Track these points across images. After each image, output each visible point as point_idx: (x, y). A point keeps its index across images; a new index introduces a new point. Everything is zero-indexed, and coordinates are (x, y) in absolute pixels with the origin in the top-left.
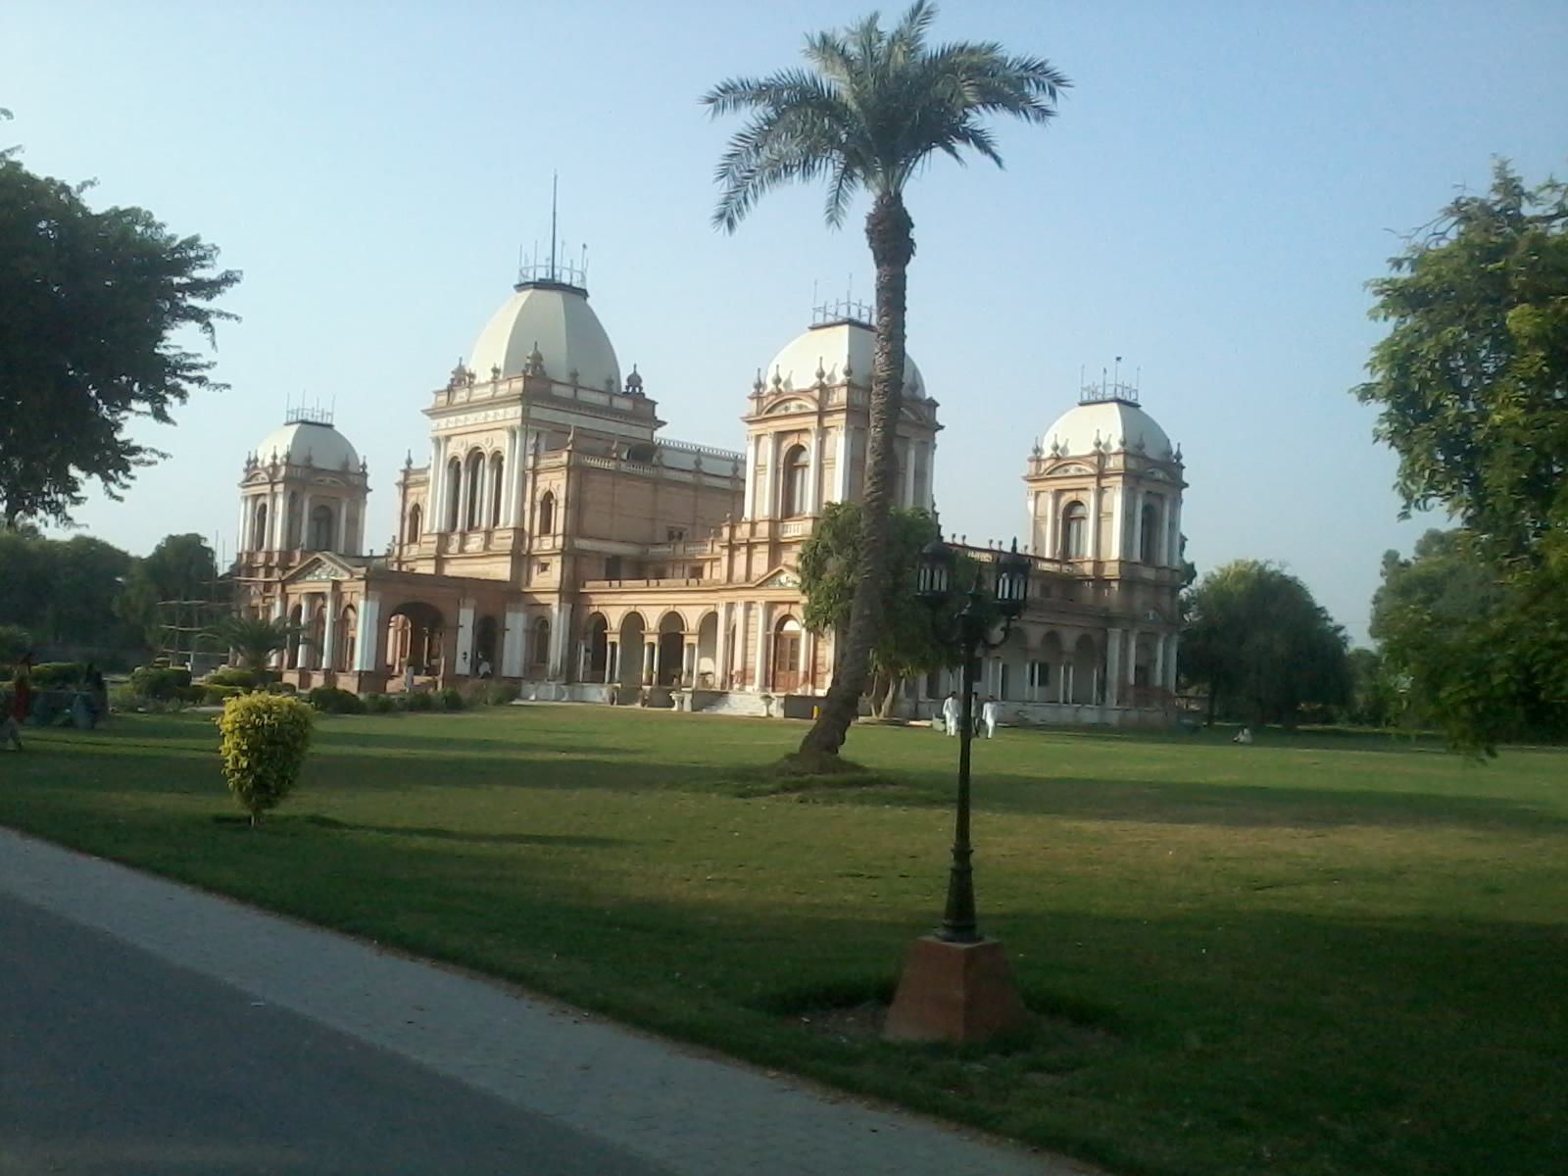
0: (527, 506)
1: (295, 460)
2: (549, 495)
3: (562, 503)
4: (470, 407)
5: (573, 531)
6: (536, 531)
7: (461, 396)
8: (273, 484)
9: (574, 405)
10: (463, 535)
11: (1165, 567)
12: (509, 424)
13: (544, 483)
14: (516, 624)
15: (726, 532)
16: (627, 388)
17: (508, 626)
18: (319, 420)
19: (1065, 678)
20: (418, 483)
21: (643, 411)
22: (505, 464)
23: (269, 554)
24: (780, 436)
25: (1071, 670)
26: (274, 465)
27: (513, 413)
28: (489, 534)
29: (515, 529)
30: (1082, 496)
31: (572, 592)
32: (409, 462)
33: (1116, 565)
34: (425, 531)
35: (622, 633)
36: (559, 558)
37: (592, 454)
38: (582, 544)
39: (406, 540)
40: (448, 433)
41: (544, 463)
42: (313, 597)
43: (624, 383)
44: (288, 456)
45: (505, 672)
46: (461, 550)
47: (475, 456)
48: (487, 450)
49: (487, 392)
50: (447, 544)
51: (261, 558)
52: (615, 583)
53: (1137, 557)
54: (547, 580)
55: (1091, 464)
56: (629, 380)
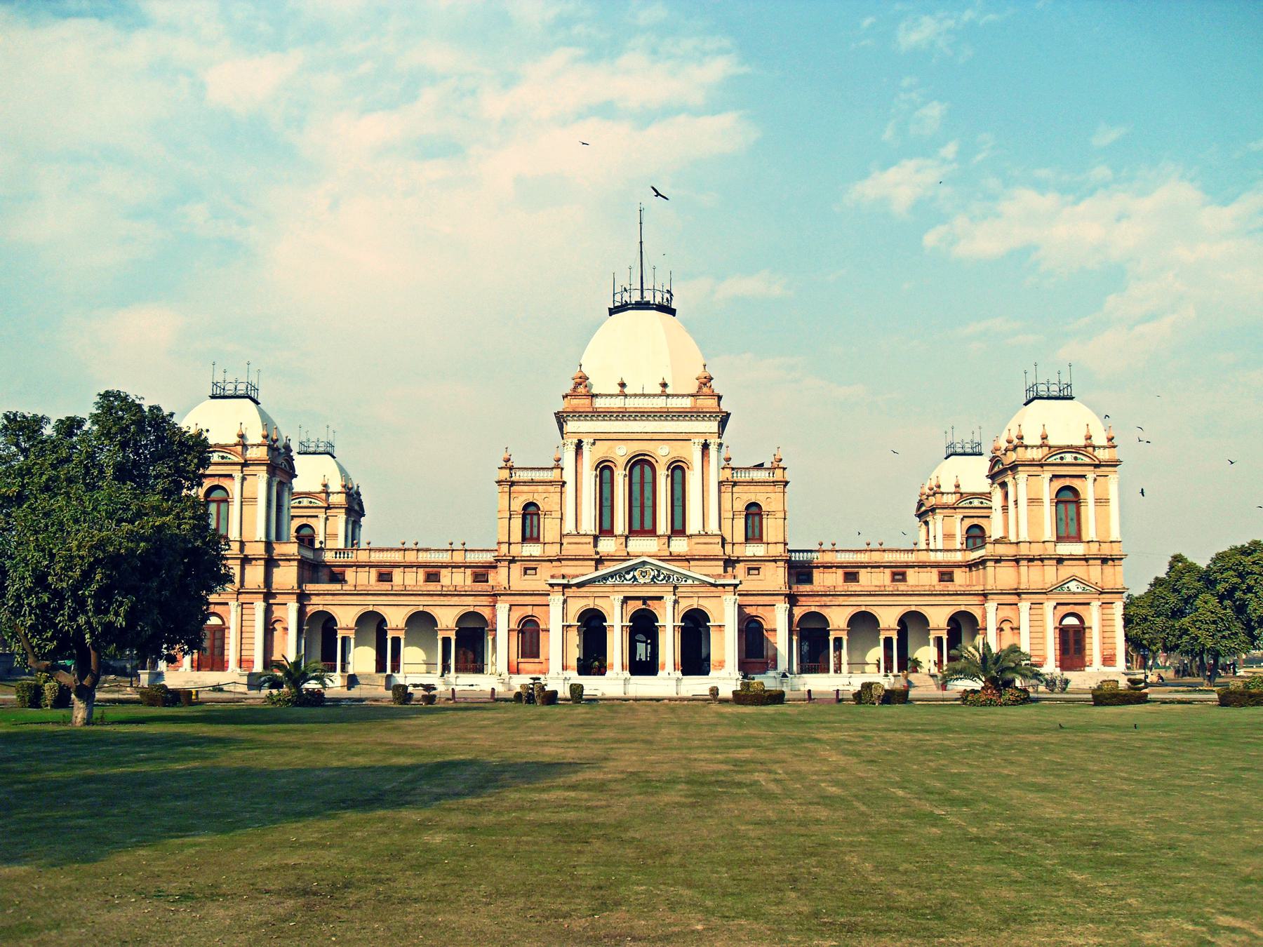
6: (740, 536)
13: (745, 496)
24: (1055, 477)
31: (792, 599)
39: (517, 535)
50: (595, 546)
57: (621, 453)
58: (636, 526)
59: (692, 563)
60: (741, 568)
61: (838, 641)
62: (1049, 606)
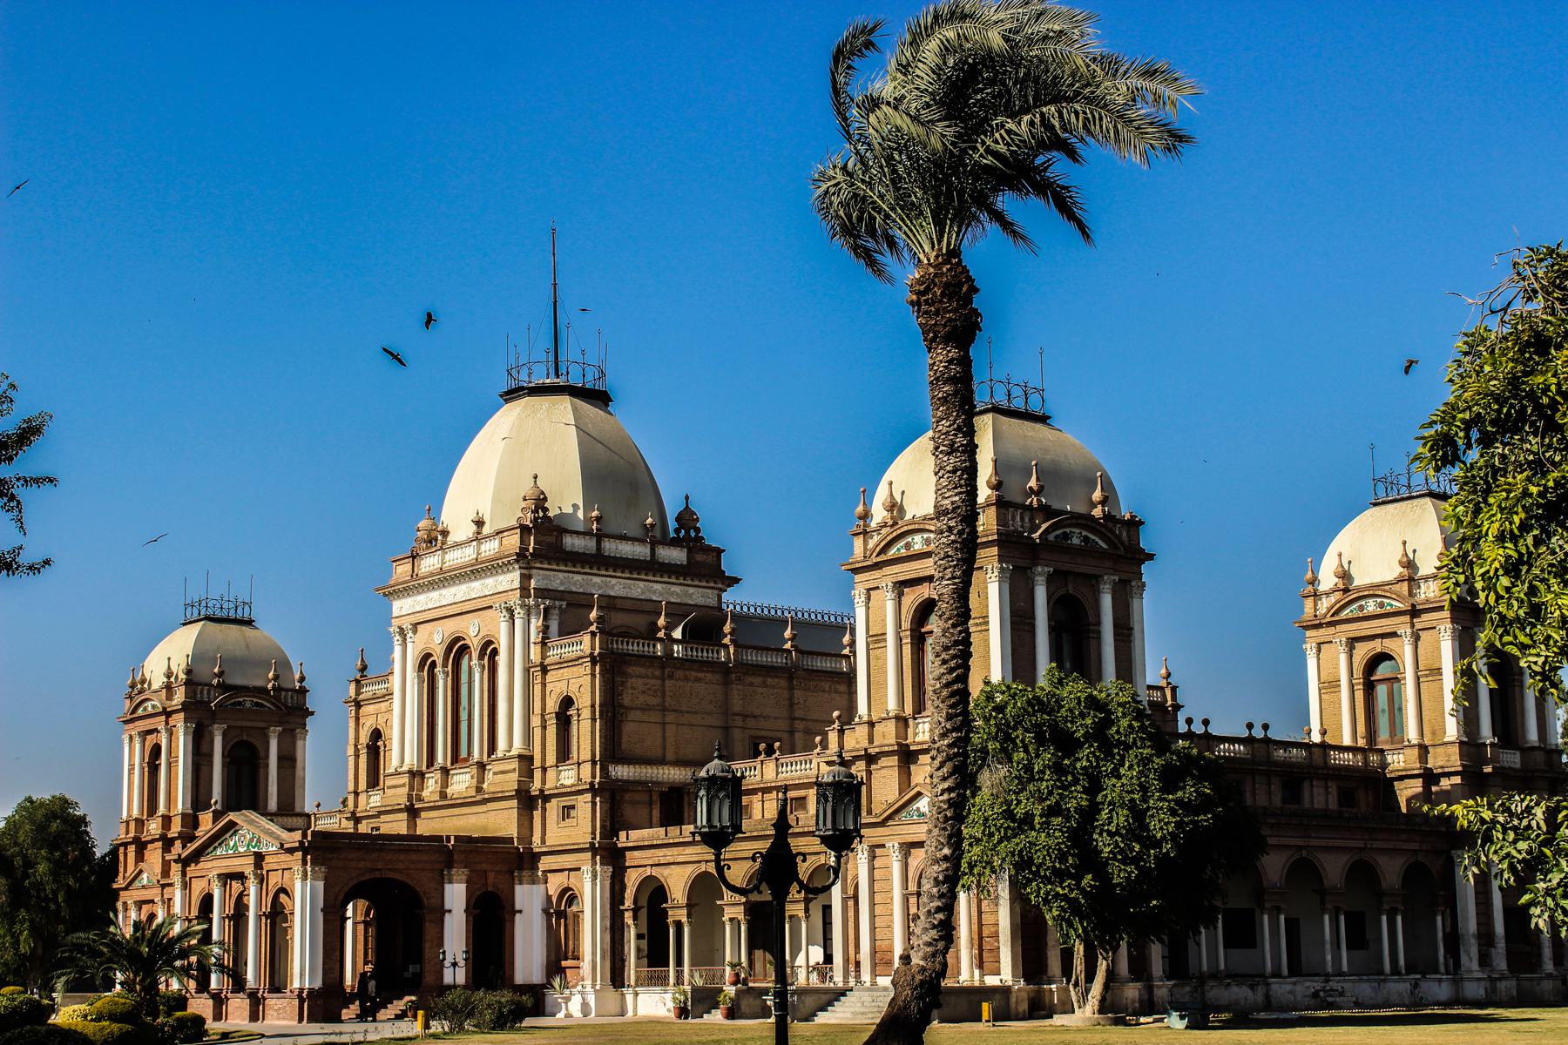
0: (536, 721)
1: (203, 673)
2: (567, 702)
3: (586, 713)
4: (444, 578)
5: (612, 751)
7: (429, 564)
8: (168, 714)
9: (599, 561)
10: (445, 771)
11: (1533, 748)
12: (501, 599)
14: (529, 899)
15: (833, 737)
16: (677, 531)
17: (518, 907)
18: (232, 614)
19: (1391, 935)
20: (376, 699)
21: (706, 564)
22: (502, 659)
23: (167, 820)
24: (901, 586)
25: (1399, 919)
26: (169, 687)
27: (511, 579)
28: (482, 766)
29: (520, 756)
30: (1389, 645)
31: (611, 856)
32: (364, 668)
33: (1456, 749)
34: (392, 770)
35: (690, 906)
36: (588, 796)
37: (626, 634)
38: (621, 772)
40: (415, 619)
41: (554, 655)
42: (227, 878)
43: (672, 524)
44: (189, 672)
45: (519, 979)
46: (443, 795)
47: (457, 649)
48: (475, 644)
49: (467, 555)
51: (154, 827)
52: (674, 831)
53: (1486, 733)
54: (570, 827)
55: (1400, 598)
56: (677, 519)
57: (437, 639)
58: (463, 754)
59: (491, 806)
60: (553, 807)
61: (679, 925)
62: (893, 846)
